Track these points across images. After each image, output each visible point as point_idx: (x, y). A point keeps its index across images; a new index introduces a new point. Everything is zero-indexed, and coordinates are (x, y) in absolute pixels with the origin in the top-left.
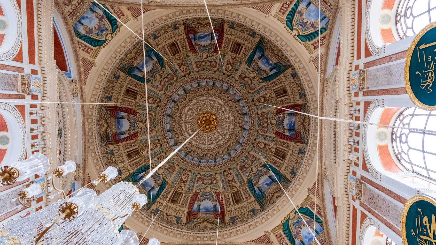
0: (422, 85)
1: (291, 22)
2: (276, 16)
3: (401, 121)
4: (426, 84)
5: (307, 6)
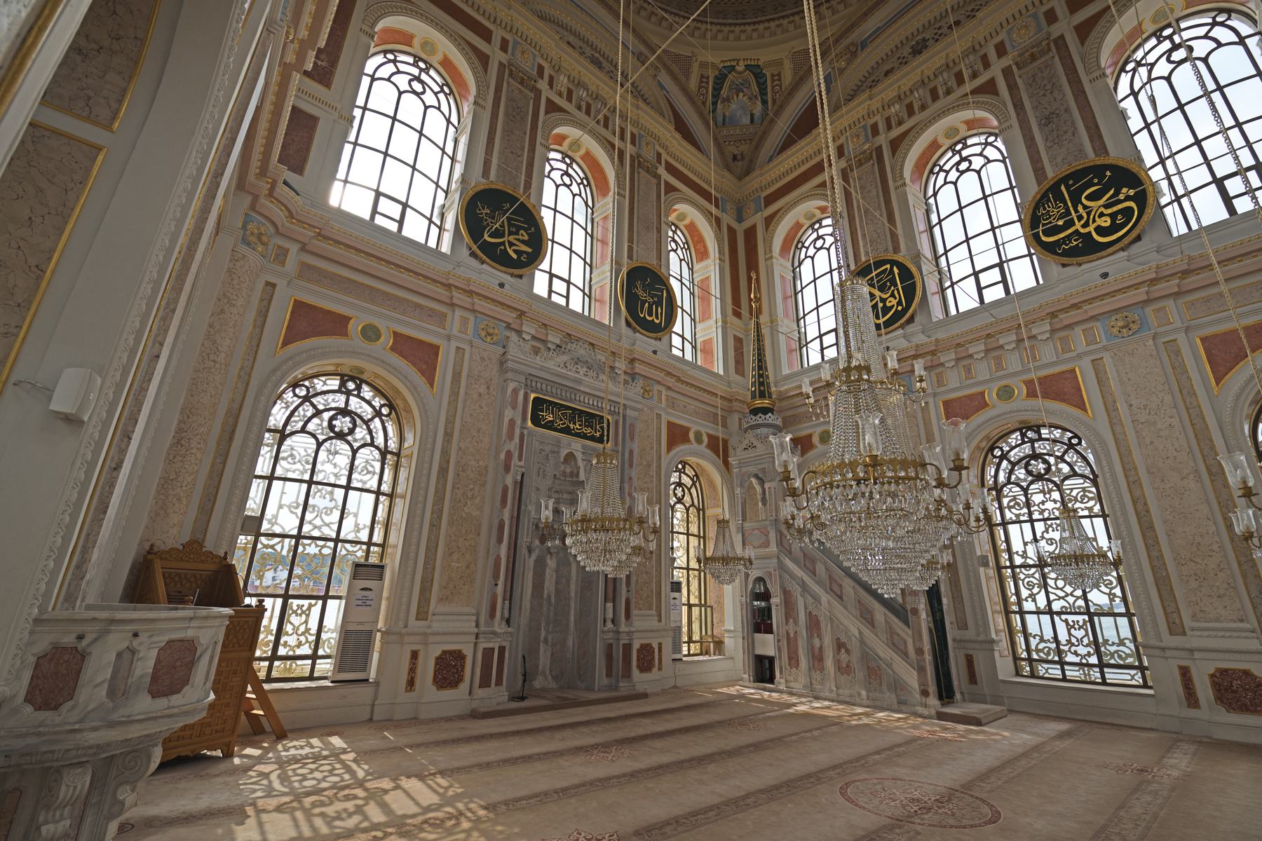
1: (756, 75)
2: (779, 63)
5: (752, 115)
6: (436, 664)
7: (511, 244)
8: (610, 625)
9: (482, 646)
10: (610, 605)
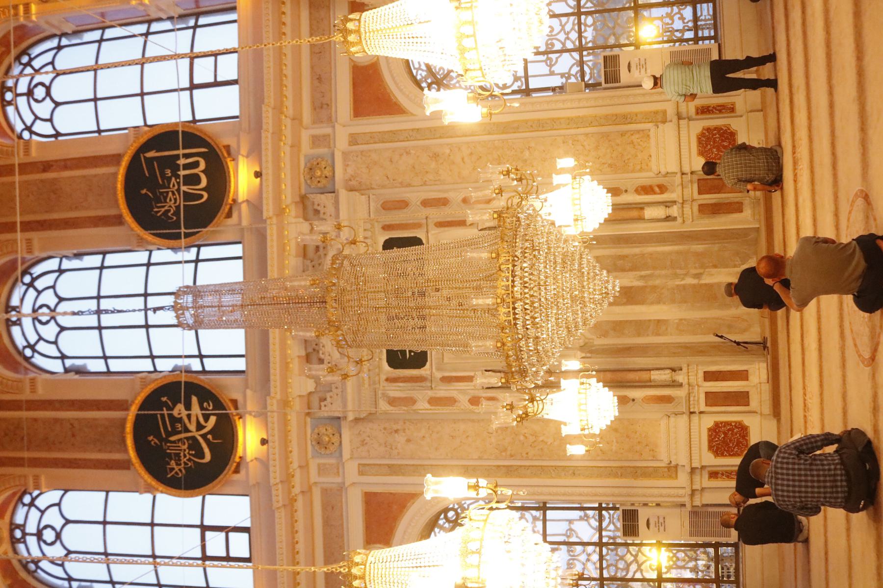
0: (156, 210)
3: (31, 285)
4: (163, 210)
6: (722, 455)
7: (200, 427)
8: (674, 211)
9: (703, 407)
10: (649, 213)
